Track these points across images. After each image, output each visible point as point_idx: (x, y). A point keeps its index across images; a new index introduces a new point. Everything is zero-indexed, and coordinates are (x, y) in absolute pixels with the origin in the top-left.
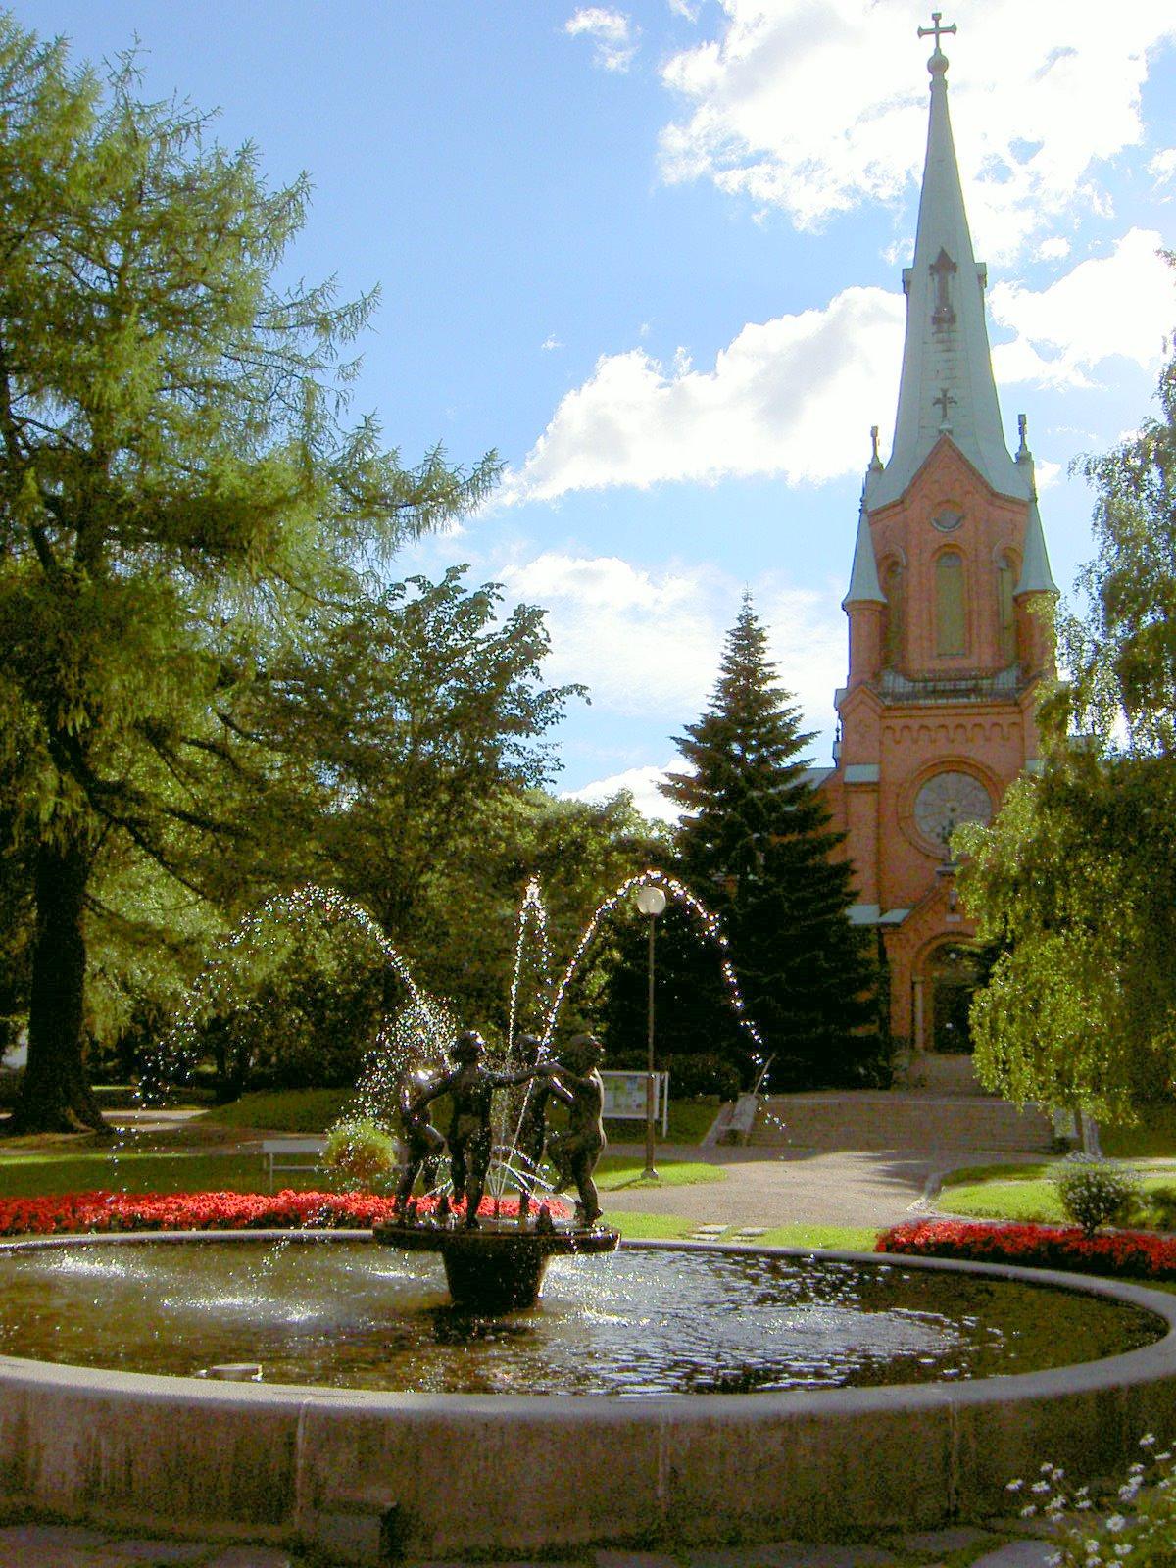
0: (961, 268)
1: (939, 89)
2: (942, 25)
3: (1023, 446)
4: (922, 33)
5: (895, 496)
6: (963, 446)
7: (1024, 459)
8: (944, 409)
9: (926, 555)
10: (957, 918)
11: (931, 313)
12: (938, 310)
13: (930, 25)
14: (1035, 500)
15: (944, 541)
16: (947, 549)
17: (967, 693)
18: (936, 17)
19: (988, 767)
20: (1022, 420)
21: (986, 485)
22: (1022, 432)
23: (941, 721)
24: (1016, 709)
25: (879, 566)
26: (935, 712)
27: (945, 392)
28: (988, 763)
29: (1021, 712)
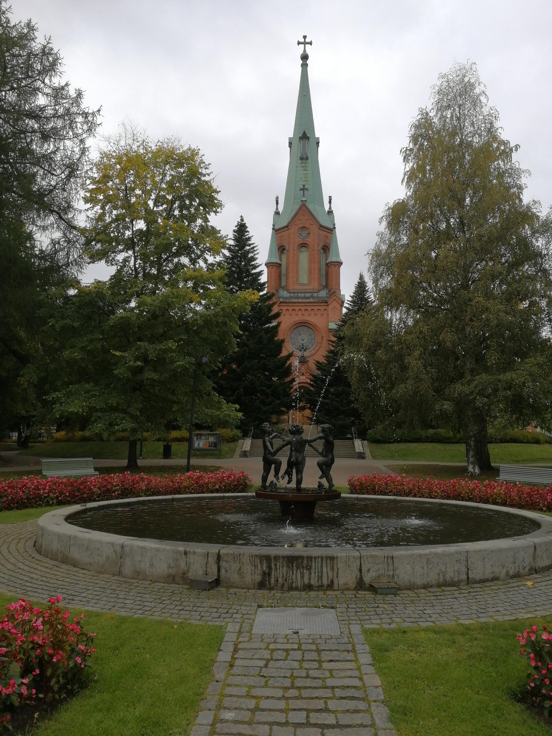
0: (310, 139)
1: (304, 66)
2: (307, 40)
3: (330, 208)
4: (299, 43)
5: (285, 224)
6: (310, 206)
7: (330, 212)
8: (304, 192)
9: (296, 247)
10: (304, 377)
11: (299, 155)
13: (302, 40)
14: (335, 228)
15: (302, 242)
17: (308, 298)
18: (305, 37)
20: (330, 197)
21: (318, 222)
22: (330, 202)
25: (278, 250)
27: (304, 186)
28: (316, 323)
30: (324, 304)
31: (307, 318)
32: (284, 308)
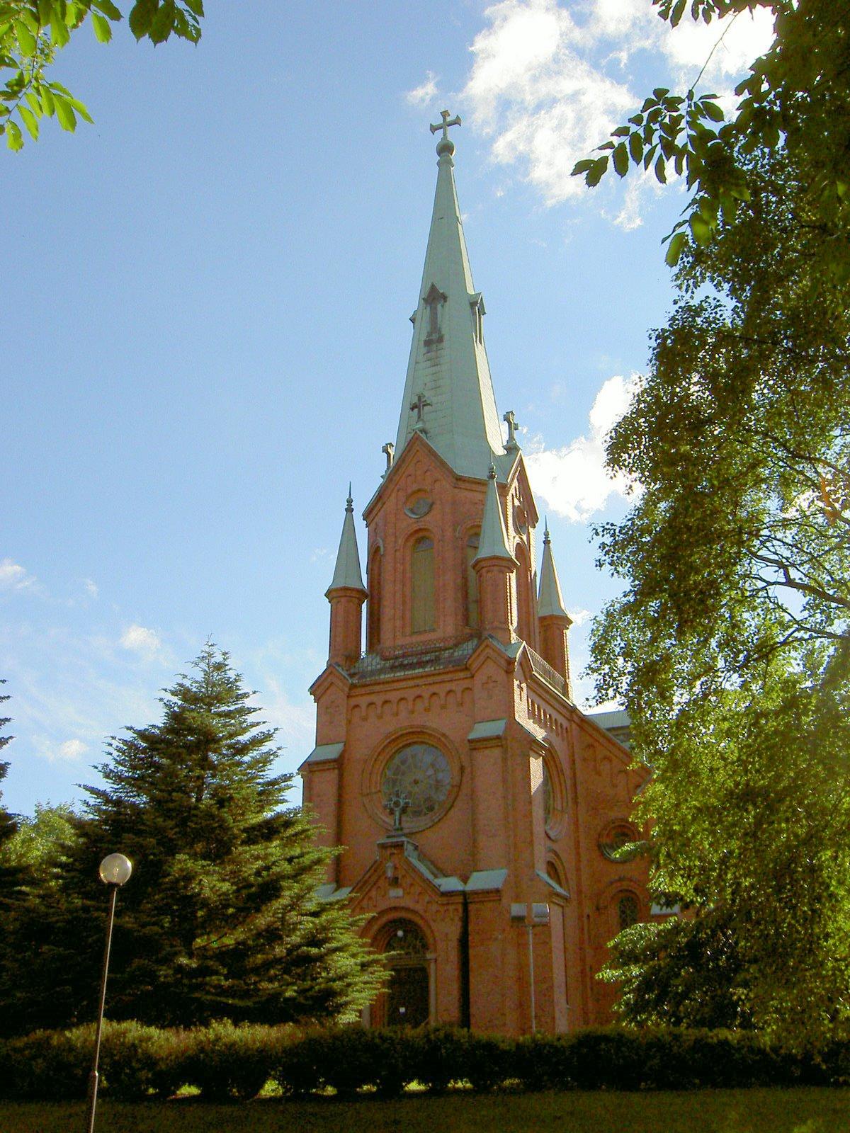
2: (449, 119)
4: (434, 129)
10: (399, 892)
11: (424, 337)
12: (430, 334)
15: (416, 527)
16: (421, 534)
19: (444, 735)
21: (451, 471)
23: (399, 694)
24: (467, 674)
26: (395, 685)
28: (445, 731)
29: (473, 677)
30: (462, 675)
31: (420, 720)
32: (363, 701)
